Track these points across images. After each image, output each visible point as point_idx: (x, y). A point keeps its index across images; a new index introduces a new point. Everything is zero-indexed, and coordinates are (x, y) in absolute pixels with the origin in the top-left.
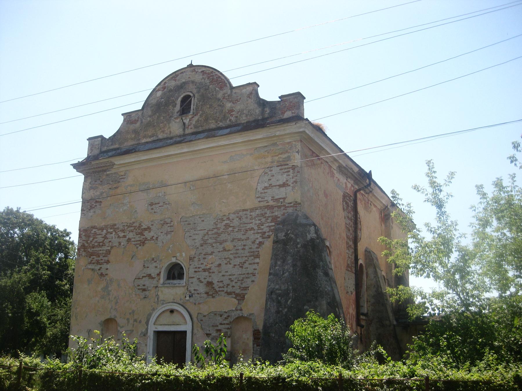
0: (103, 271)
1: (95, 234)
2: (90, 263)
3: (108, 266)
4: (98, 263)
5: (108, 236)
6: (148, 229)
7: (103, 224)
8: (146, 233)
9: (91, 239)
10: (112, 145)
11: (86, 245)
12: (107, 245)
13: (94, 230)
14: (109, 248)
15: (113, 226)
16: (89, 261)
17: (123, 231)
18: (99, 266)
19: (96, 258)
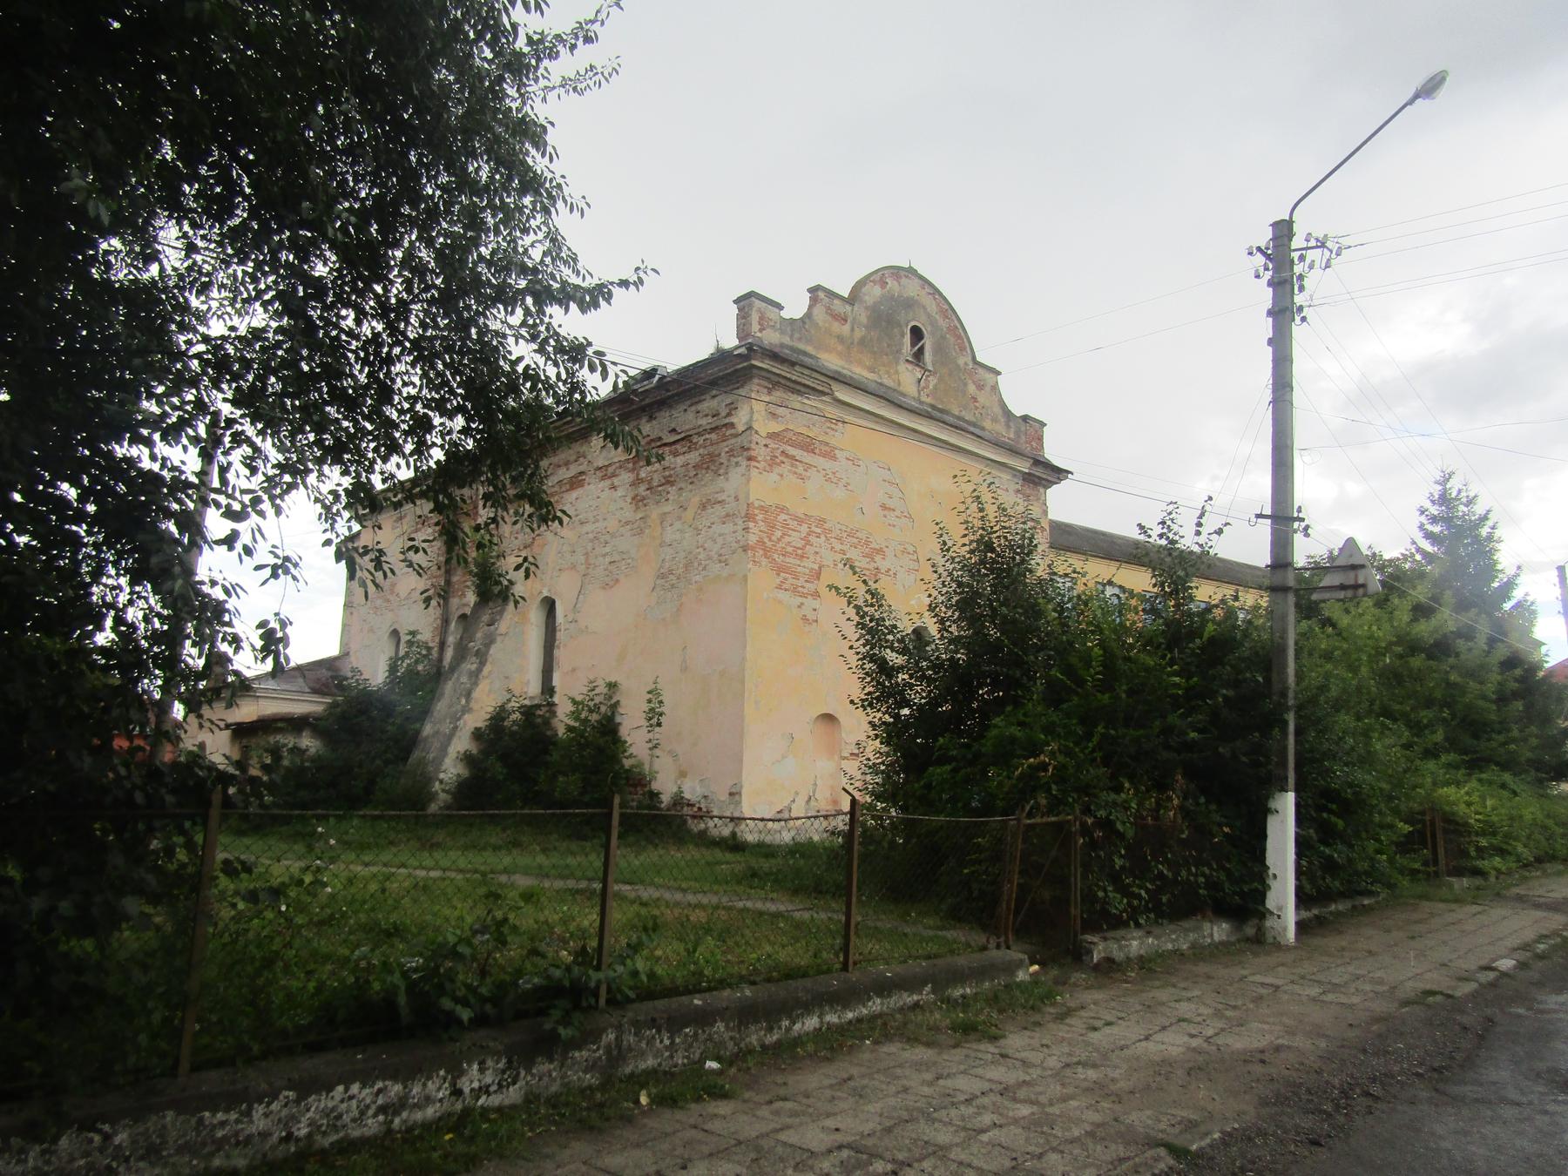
0: (806, 611)
1: (785, 525)
2: (779, 587)
3: (816, 604)
4: (795, 590)
5: (812, 539)
6: (880, 551)
7: (800, 512)
8: (878, 558)
9: (778, 534)
10: (800, 339)
11: (769, 544)
12: (812, 558)
13: (783, 517)
14: (816, 567)
15: (821, 521)
16: (778, 581)
17: (839, 539)
18: (801, 600)
19: (791, 581)
